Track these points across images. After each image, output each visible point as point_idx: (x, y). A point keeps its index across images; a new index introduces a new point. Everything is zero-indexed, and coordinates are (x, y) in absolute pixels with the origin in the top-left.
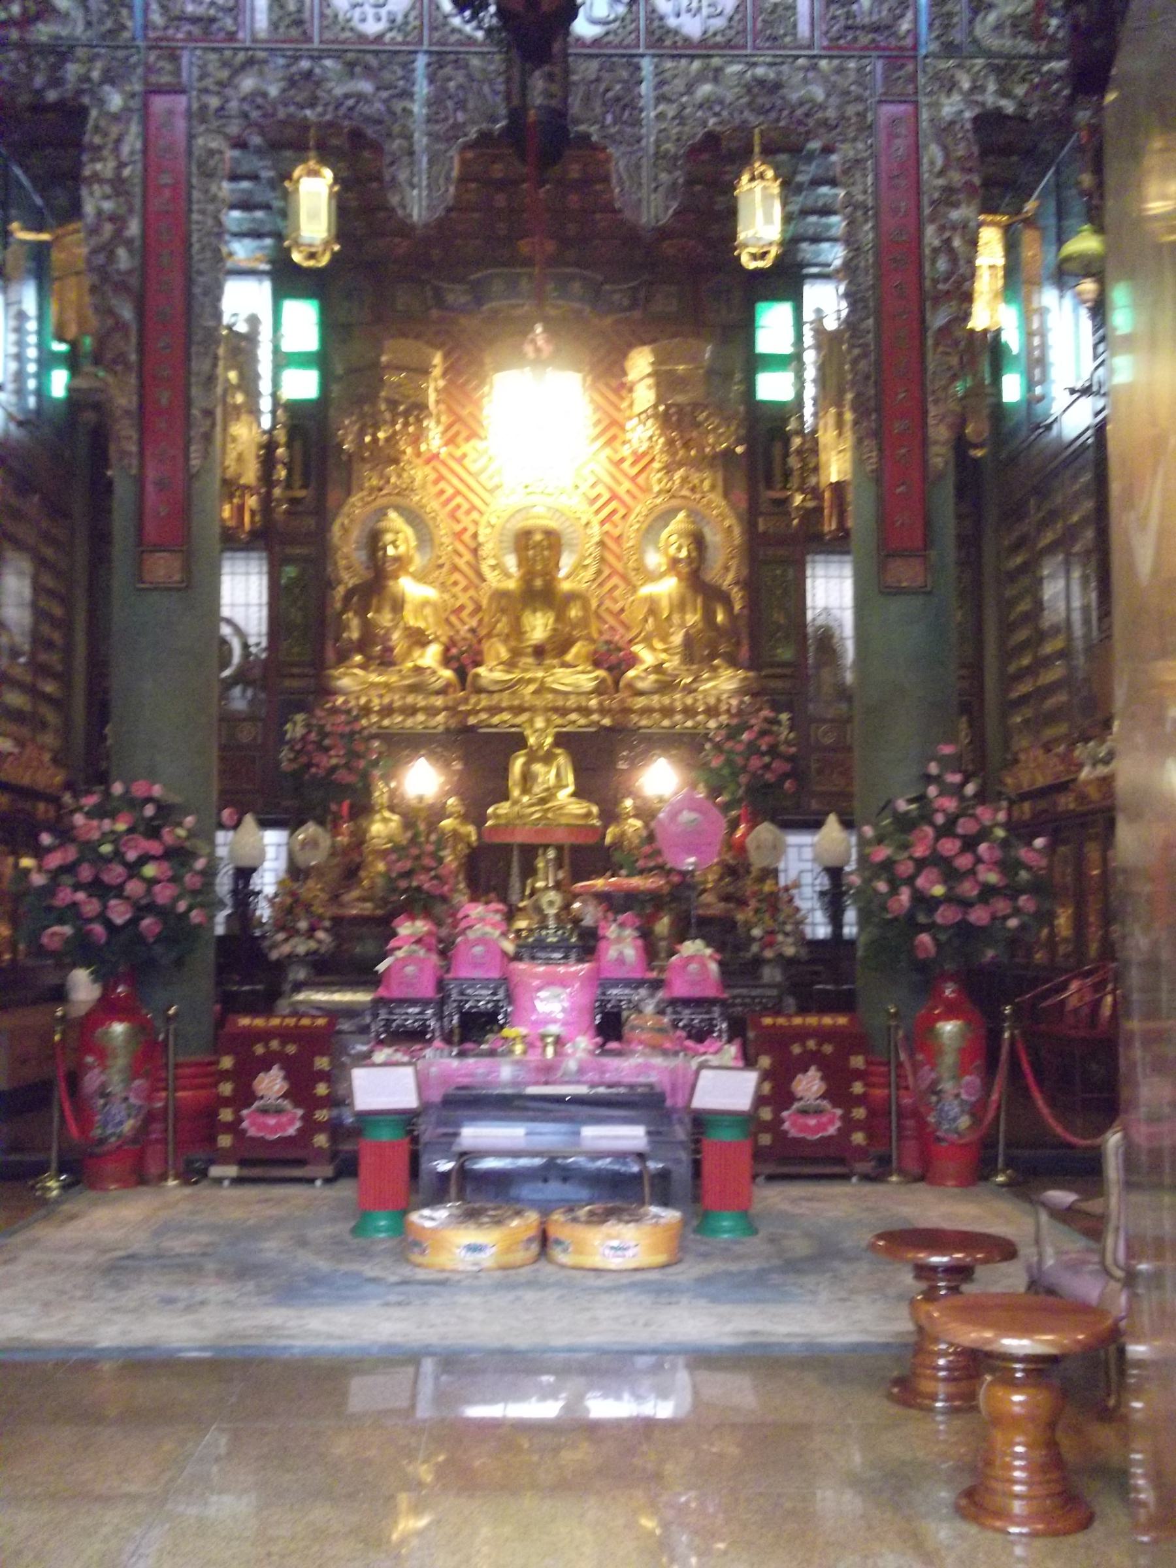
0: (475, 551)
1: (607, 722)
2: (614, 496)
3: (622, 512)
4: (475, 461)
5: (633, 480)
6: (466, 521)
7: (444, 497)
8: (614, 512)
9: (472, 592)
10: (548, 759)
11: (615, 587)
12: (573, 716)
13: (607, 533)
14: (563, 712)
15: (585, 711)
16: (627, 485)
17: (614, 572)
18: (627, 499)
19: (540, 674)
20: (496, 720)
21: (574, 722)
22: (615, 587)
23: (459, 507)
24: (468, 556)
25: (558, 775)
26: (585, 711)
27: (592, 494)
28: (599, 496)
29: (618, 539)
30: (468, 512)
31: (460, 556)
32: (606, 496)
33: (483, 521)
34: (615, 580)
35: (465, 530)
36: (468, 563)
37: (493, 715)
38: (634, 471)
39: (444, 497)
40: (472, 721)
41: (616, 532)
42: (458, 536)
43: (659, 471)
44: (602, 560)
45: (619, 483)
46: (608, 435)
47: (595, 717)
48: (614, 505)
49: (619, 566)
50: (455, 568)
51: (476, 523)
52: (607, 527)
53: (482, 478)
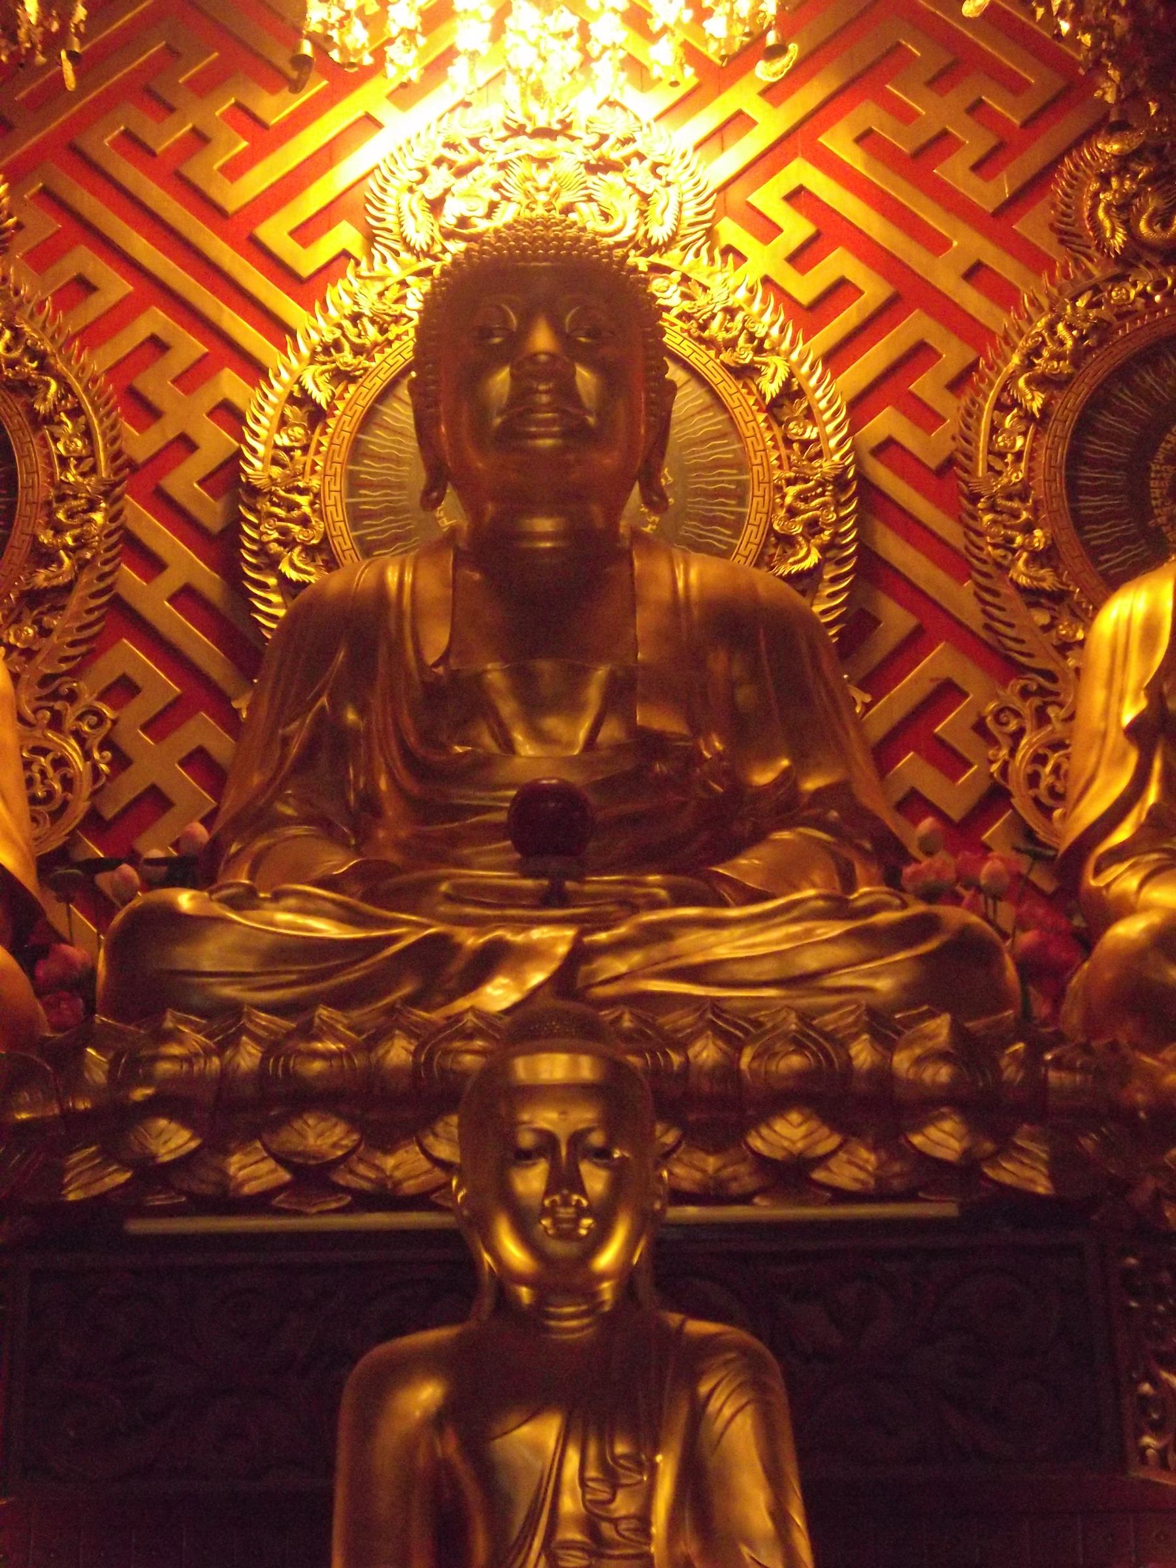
0: (223, 547)
1: (1027, 1172)
2: (907, 293)
3: (953, 355)
4: (235, 170)
5: (996, 222)
6: (187, 414)
7: (93, 308)
8: (919, 355)
9: (202, 731)
10: (622, 1387)
11: (946, 693)
12: (788, 1133)
13: (887, 448)
14: (722, 1110)
15: (867, 1108)
16: (968, 244)
17: (932, 622)
18: (972, 301)
19: (557, 939)
20: (252, 1170)
21: (791, 1175)
22: (946, 693)
23: (157, 346)
24: (186, 564)
25: (700, 1488)
26: (867, 1108)
27: (805, 287)
28: (841, 290)
29: (946, 478)
30: (193, 378)
31: (151, 564)
32: (873, 290)
33: (265, 410)
34: (939, 662)
35: (185, 444)
36: (186, 597)
37: (216, 1143)
38: (989, 194)
39: (93, 308)
40: (88, 1178)
41: (930, 447)
42: (142, 478)
43: (1123, 164)
44: (872, 570)
45: (937, 244)
46: (866, 51)
47: (943, 1138)
48: (916, 326)
49: (961, 598)
50: (124, 617)
51: (230, 415)
52: (886, 423)
53: (275, 233)
